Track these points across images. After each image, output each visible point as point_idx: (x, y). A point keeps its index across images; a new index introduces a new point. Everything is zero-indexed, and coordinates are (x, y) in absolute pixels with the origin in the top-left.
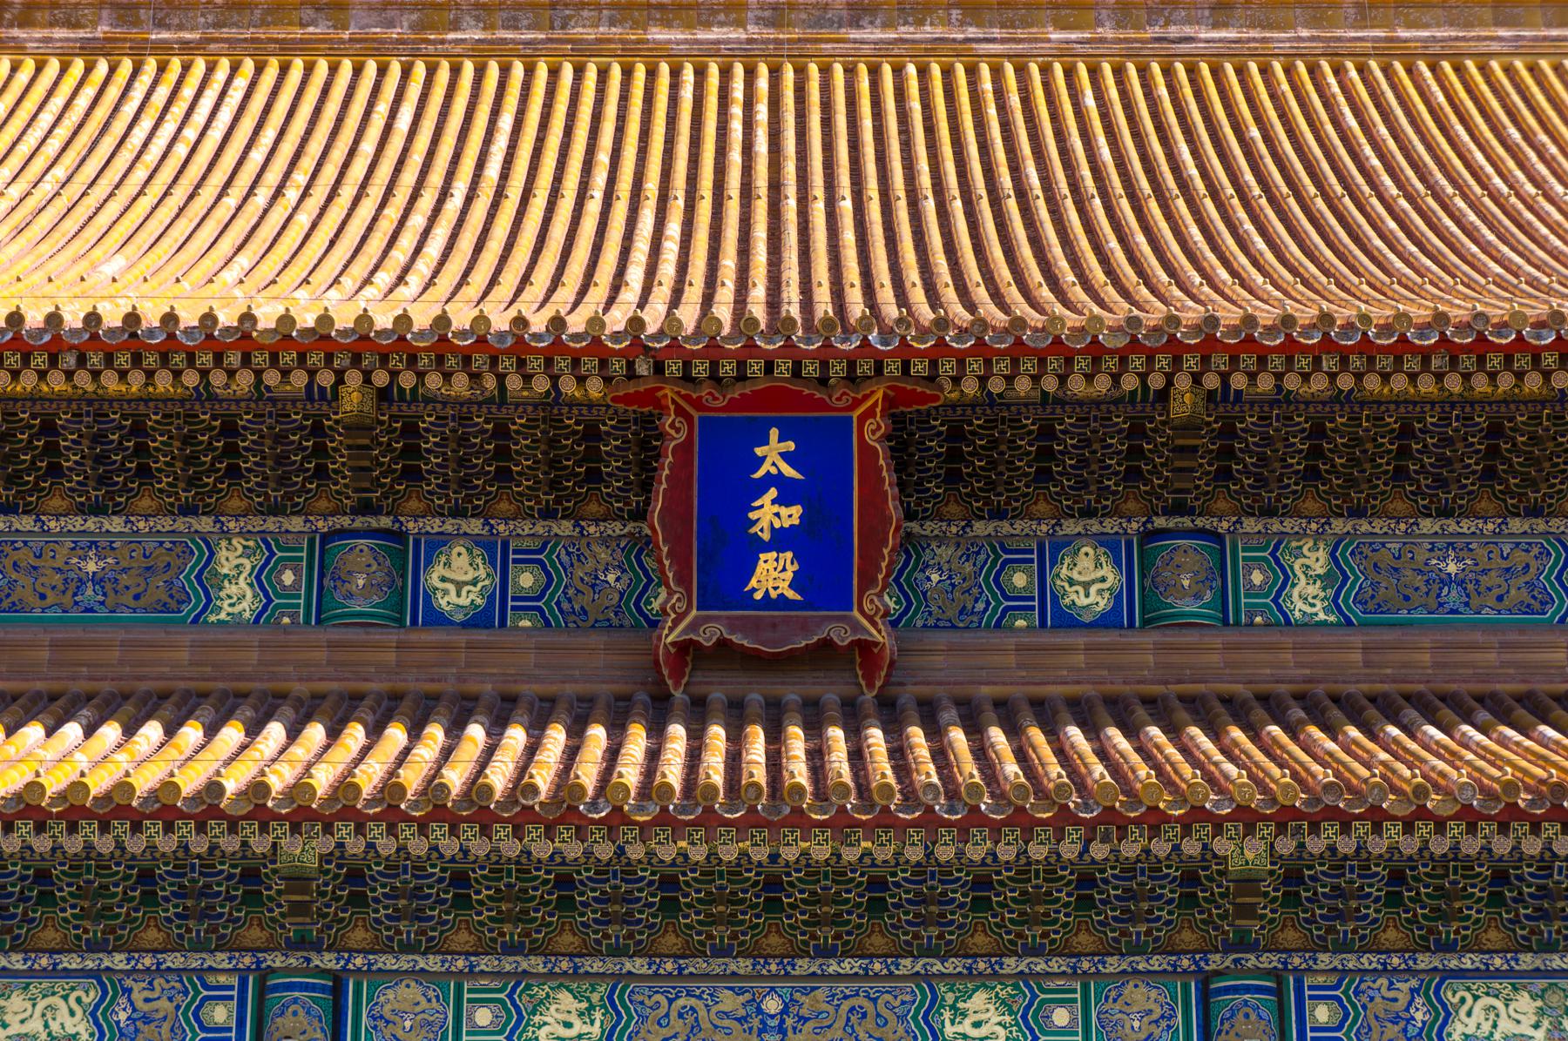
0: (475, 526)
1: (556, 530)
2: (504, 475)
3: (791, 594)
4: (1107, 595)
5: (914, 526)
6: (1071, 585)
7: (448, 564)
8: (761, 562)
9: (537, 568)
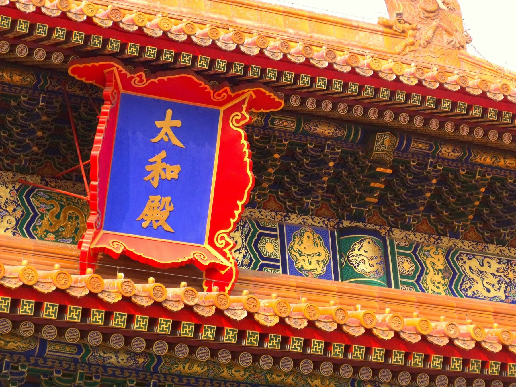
4: (322, 264)
6: (300, 255)
8: (149, 203)
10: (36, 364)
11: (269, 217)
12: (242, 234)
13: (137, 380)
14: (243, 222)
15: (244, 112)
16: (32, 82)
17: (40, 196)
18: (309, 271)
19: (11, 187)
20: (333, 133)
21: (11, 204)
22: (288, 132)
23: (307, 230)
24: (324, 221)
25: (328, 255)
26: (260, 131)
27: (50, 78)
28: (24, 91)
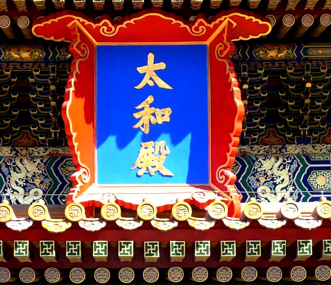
3: (165, 172)
5: (246, 148)
11: (323, 151)
12: (289, 171)
14: (290, 159)
15: (225, 41)
16: (41, 55)
17: (69, 166)
19: (38, 161)
21: (38, 178)
22: (327, 60)
26: (294, 64)
27: (58, 49)
28: (36, 65)
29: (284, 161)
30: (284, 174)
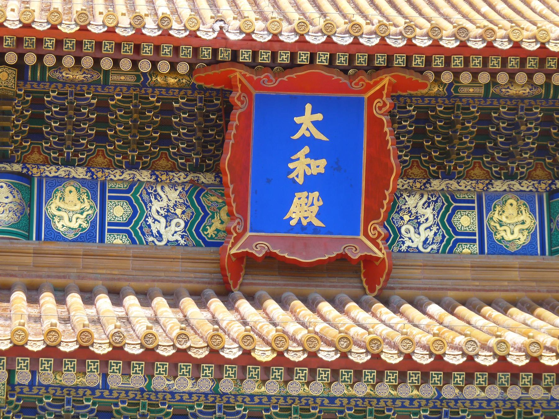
0: (80, 173)
1: (138, 177)
2: (101, 138)
3: (317, 223)
4: (526, 233)
6: (501, 225)
7: (62, 199)
8: (296, 200)
9: (125, 204)
10: (102, 397)
12: (434, 209)
13: (205, 403)
14: (435, 197)
15: (384, 98)
17: (211, 195)
18: (510, 241)
19: (180, 189)
20: (529, 92)
22: (477, 98)
23: (510, 197)
24: (533, 184)
25: (533, 221)
26: (444, 101)
28: (182, 93)
29: (429, 199)
30: (429, 213)
